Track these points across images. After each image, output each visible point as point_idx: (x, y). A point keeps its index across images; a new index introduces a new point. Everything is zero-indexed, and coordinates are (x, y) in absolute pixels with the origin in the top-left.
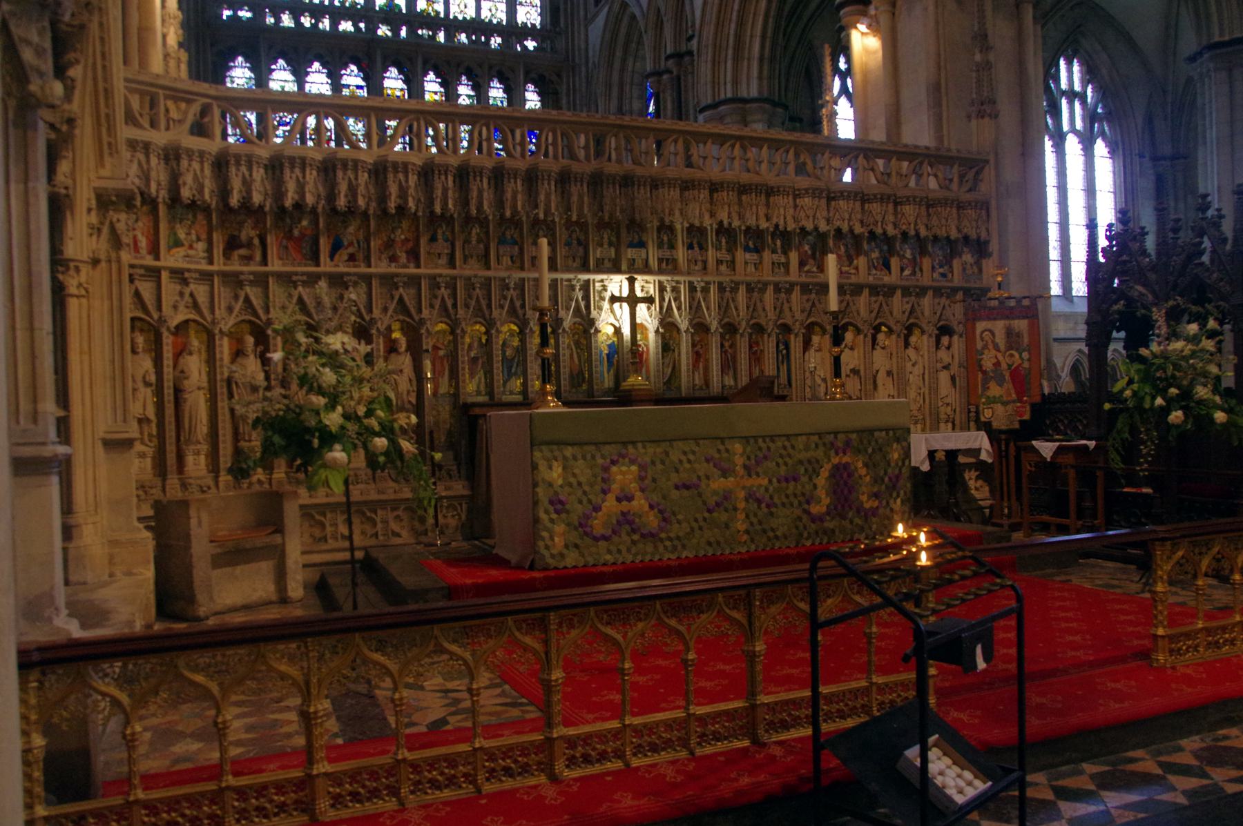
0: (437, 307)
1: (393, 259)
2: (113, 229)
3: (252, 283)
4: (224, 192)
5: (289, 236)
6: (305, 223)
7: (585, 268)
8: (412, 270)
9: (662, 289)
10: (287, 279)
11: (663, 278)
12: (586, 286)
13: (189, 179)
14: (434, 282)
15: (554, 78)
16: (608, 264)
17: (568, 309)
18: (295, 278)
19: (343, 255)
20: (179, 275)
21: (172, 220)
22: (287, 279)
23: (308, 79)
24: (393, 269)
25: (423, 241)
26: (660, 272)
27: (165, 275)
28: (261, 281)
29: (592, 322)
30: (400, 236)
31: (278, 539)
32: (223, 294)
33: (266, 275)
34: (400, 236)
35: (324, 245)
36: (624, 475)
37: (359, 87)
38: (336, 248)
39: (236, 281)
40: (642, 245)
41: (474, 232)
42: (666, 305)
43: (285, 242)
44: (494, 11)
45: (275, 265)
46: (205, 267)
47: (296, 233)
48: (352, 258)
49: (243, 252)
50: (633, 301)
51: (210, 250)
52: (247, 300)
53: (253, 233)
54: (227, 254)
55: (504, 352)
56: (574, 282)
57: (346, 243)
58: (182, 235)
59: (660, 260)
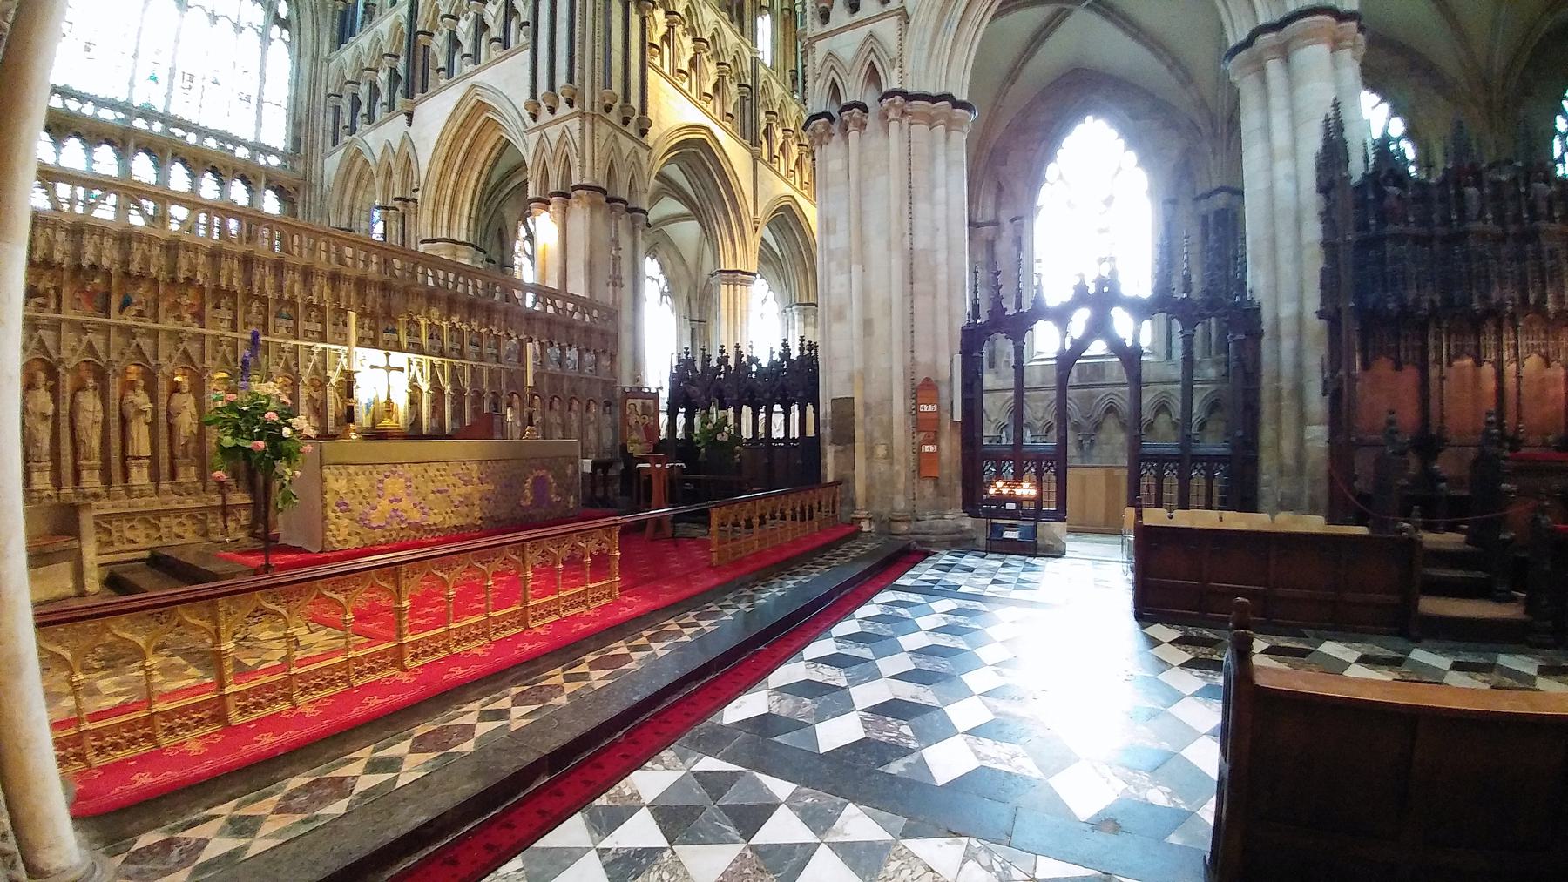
0: (219, 358)
1: (179, 318)
3: (46, 327)
5: (82, 290)
6: (97, 281)
8: (197, 329)
9: (410, 363)
10: (80, 328)
14: (217, 342)
15: (292, 190)
17: (335, 370)
18: (87, 326)
19: (133, 310)
22: (80, 328)
24: (179, 326)
25: (208, 307)
26: (407, 351)
28: (56, 326)
30: (185, 300)
31: (76, 544)
35: (115, 302)
36: (395, 486)
38: (126, 304)
40: (394, 331)
41: (254, 304)
42: (412, 373)
43: (77, 295)
45: (68, 314)
47: (89, 288)
48: (140, 314)
49: (40, 300)
52: (41, 341)
53: (49, 285)
56: (340, 352)
57: (135, 301)
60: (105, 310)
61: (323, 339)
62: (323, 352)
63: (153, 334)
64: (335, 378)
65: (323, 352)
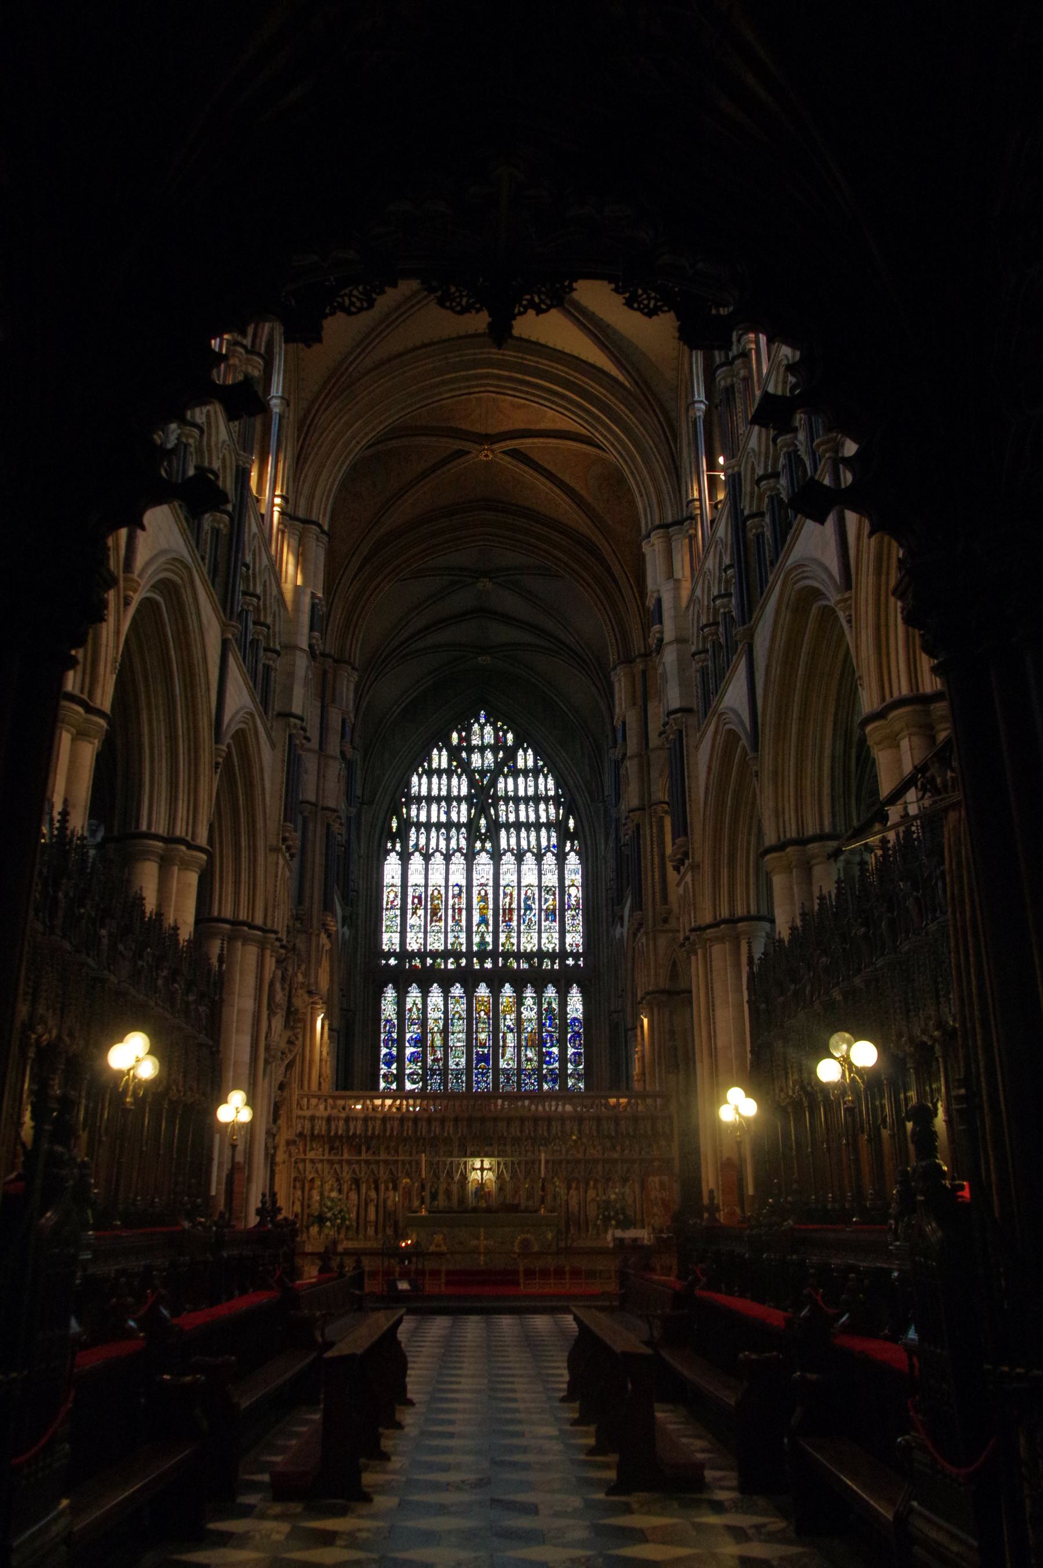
1: (389, 1153)
2: (290, 1152)
4: (329, 1130)
7: (465, 1156)
9: (499, 1164)
10: (349, 1162)
11: (499, 1159)
12: (465, 1163)
13: (317, 1127)
14: (403, 1163)
16: (476, 1153)
20: (312, 1161)
21: (311, 1141)
23: (430, 994)
24: (389, 1157)
26: (499, 1156)
27: (307, 1161)
28: (340, 1162)
29: (466, 1178)
30: (392, 1144)
32: (327, 1166)
33: (342, 1160)
34: (392, 1144)
35: (364, 1148)
36: (438, 1238)
37: (461, 997)
38: (368, 1149)
39: (331, 1162)
40: (491, 1145)
44: (550, 938)
45: (346, 1156)
46: (322, 1158)
47: (354, 1143)
48: (374, 1153)
50: (482, 1169)
51: (323, 1151)
54: (330, 1153)
55: (431, 1189)
58: (314, 1146)
59: (499, 1152)
60: (360, 1153)
61: (451, 1156)
62: (451, 1163)
63: (377, 1162)
64: (457, 1177)
65: (451, 1163)
